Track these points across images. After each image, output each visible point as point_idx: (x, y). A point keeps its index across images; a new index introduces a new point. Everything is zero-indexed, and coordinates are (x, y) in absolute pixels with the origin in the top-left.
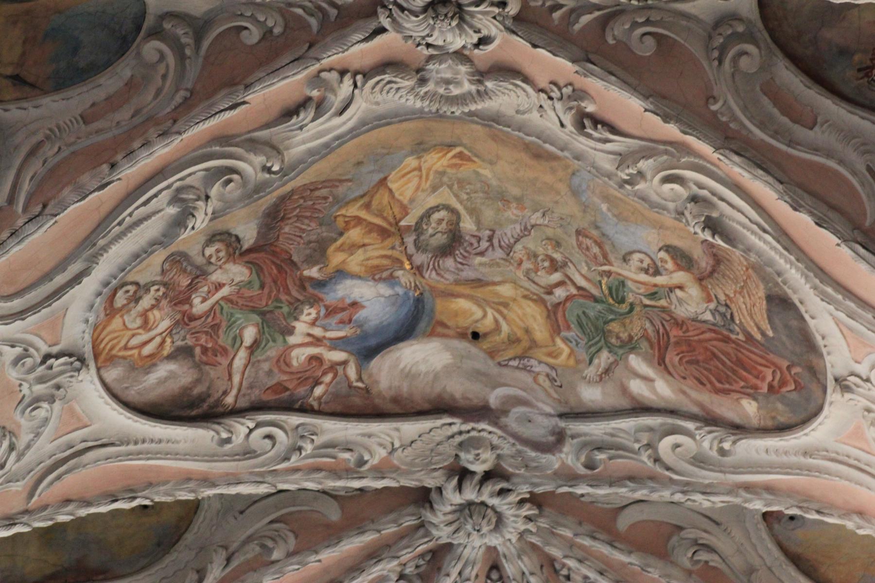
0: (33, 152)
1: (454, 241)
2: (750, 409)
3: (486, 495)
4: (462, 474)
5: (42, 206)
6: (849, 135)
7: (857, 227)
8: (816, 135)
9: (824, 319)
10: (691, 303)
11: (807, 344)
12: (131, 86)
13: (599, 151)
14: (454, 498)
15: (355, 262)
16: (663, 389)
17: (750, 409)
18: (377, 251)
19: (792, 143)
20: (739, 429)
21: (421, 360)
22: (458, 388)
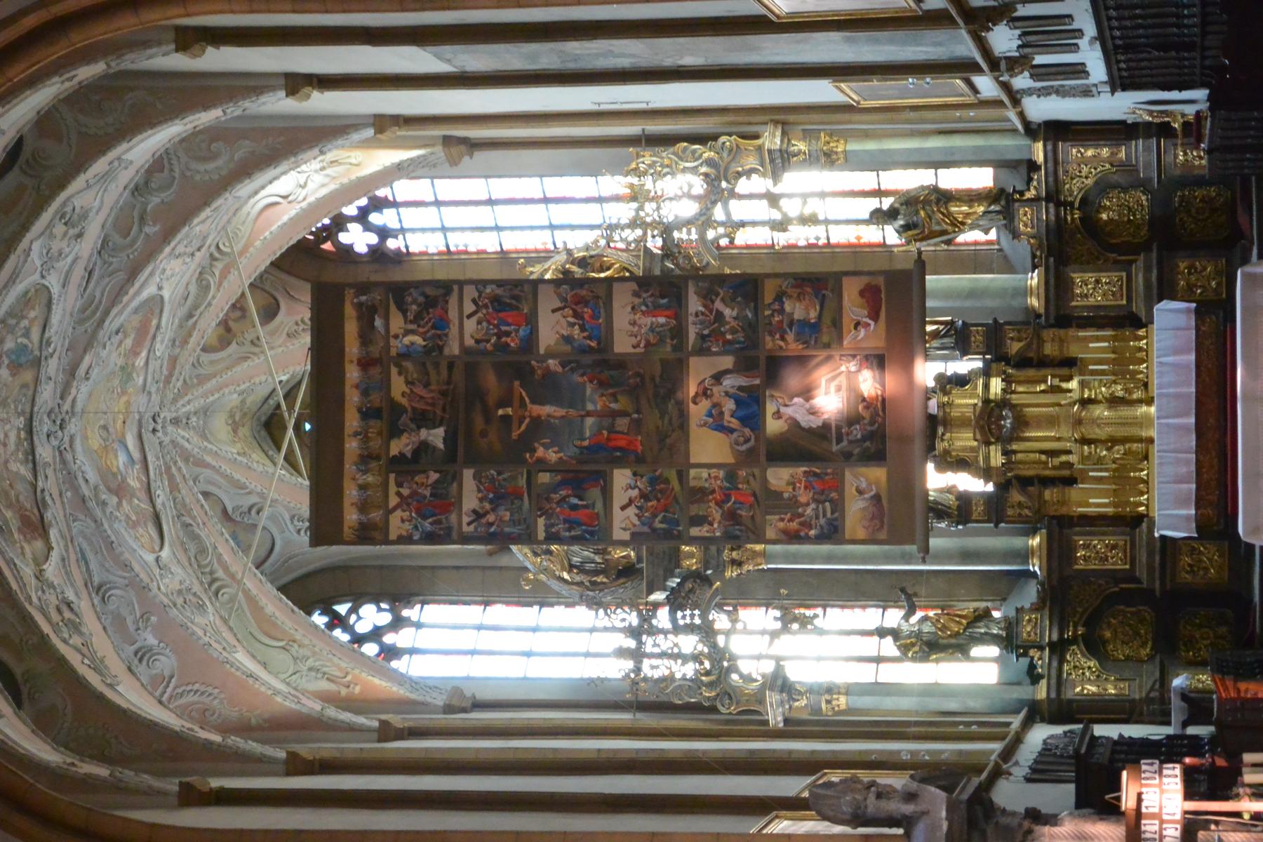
0: (108, 571)
1: (105, 428)
2: (154, 322)
3: (159, 421)
4: (154, 430)
5: (127, 566)
6: (97, 283)
7: (128, 280)
8: (98, 294)
9: (145, 294)
10: (129, 342)
11: (151, 299)
12: (85, 537)
13: (94, 374)
14: (160, 434)
15: (115, 463)
16: (144, 354)
17: (154, 322)
18: (111, 456)
19: (100, 302)
20: (158, 327)
21: (131, 441)
22: (135, 430)
